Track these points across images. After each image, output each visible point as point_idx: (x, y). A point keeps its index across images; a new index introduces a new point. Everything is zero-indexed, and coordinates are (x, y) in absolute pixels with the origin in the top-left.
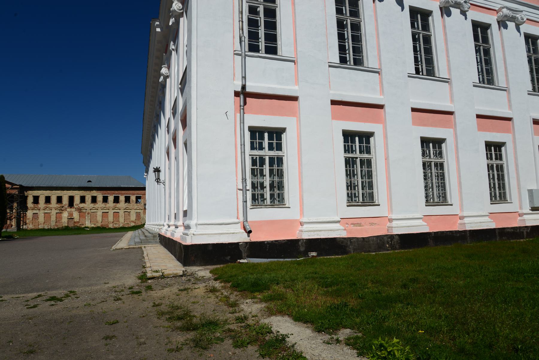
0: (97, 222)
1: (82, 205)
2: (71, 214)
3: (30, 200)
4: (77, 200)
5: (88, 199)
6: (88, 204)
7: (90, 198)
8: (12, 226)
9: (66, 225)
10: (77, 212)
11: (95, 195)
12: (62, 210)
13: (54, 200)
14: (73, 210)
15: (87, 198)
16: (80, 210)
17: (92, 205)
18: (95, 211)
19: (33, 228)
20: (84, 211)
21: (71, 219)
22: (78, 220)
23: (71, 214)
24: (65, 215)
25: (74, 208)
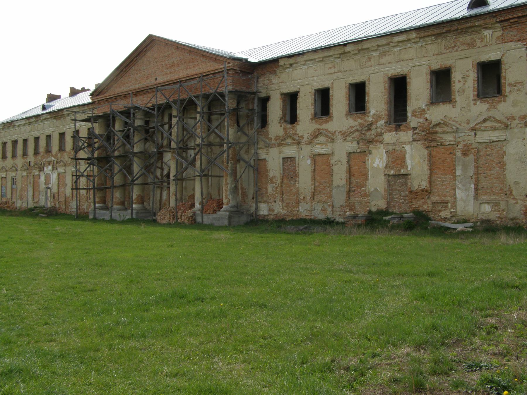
0: (509, 194)
1: (438, 113)
2: (397, 158)
3: (276, 109)
4: (419, 90)
5: (465, 79)
6: (466, 105)
7: (473, 75)
8: (220, 205)
9: (382, 205)
10: (419, 145)
11: (493, 56)
12: (367, 140)
13: (340, 101)
14: (405, 136)
15: (456, 76)
16: (429, 135)
17: (481, 108)
18: (495, 135)
19: (284, 212)
20: (448, 139)
21: (397, 177)
22: (424, 185)
23: (397, 158)
24: (378, 160)
25: (408, 129)
